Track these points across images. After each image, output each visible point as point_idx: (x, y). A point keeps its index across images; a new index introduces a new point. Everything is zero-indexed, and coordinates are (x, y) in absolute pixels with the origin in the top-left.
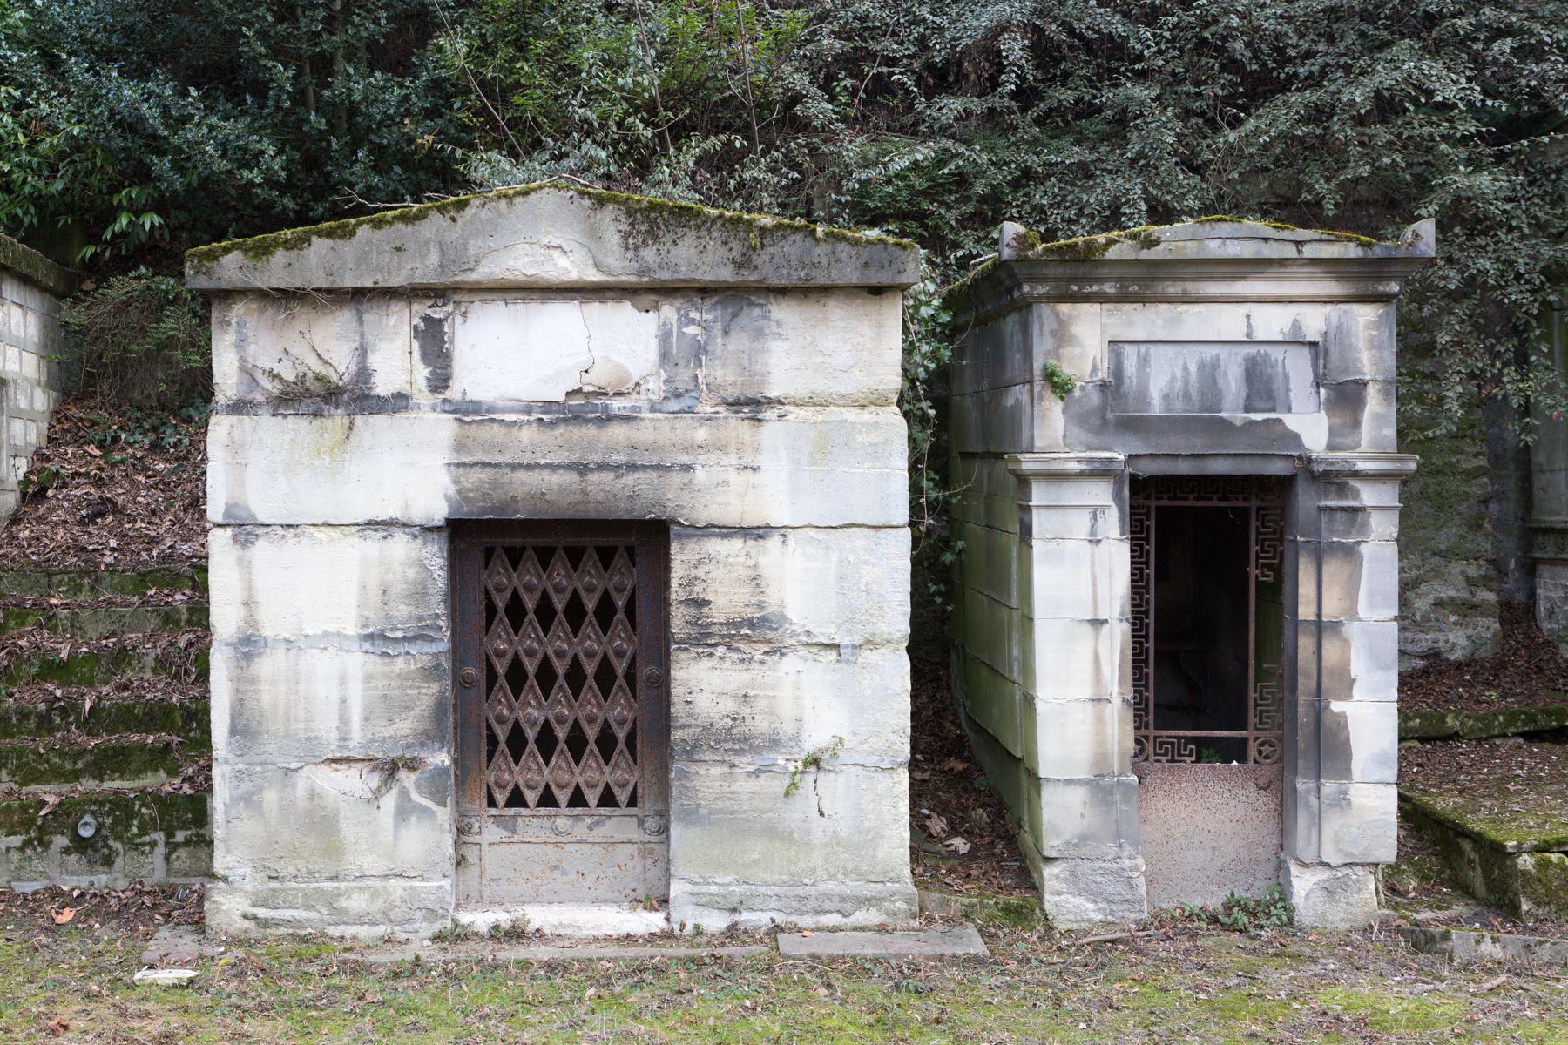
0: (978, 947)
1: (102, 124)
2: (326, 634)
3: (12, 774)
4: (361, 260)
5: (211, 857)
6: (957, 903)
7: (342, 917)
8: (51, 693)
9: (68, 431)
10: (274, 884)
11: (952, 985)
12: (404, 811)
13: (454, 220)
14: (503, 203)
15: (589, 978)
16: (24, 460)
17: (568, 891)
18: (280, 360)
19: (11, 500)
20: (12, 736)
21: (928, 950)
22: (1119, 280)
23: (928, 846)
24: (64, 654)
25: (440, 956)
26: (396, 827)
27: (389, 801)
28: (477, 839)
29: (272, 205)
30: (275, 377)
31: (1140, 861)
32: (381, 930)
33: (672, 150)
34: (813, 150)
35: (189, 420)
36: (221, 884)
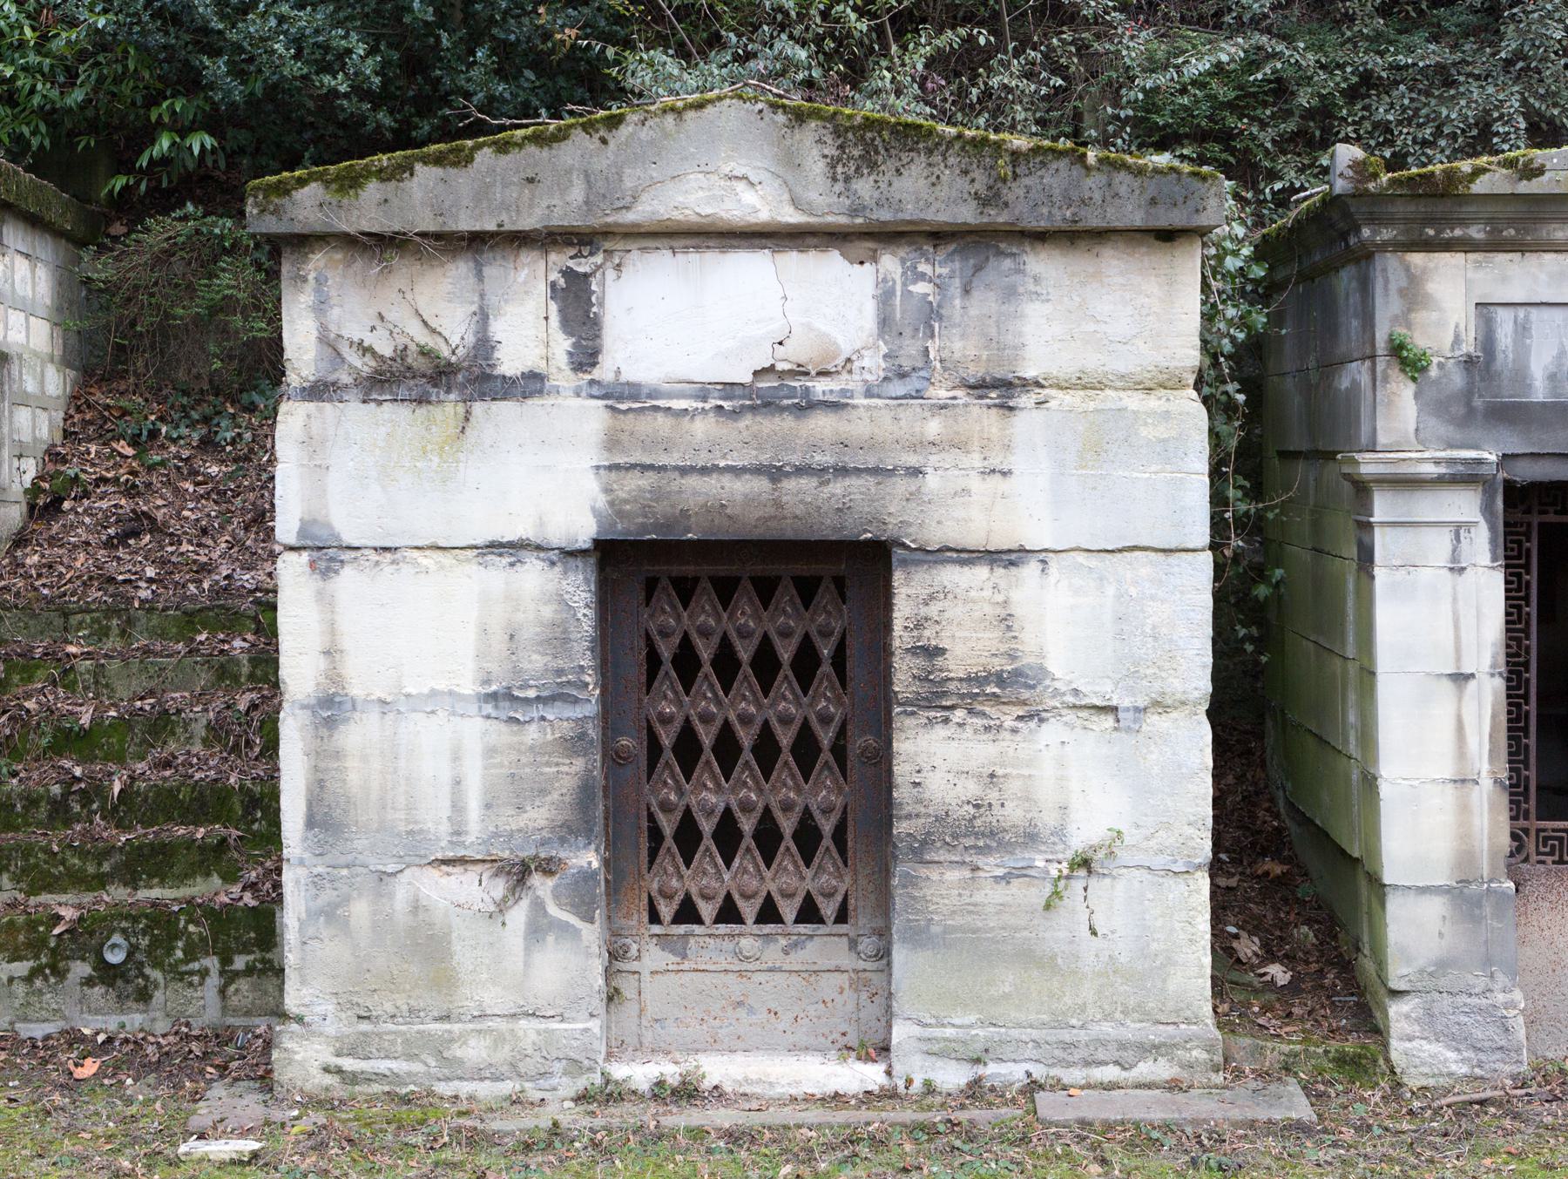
0: (1302, 1109)
1: (136, 14)
2: (434, 693)
3: (16, 879)
4: (482, 195)
5: (281, 990)
6: (1275, 1052)
7: (455, 1069)
8: (68, 771)
9: (91, 423)
10: (365, 1026)
11: (1268, 1161)
12: (538, 929)
13: (604, 141)
14: (670, 119)
15: (784, 1151)
16: (32, 461)
17: (755, 1034)
18: (373, 328)
19: (15, 514)
20: (17, 829)
21: (1236, 1114)
22: (1490, 221)
23: (1235, 976)
24: (85, 720)
25: (586, 1122)
26: (528, 950)
27: (518, 915)
28: (635, 966)
29: (362, 121)
30: (366, 350)
31: (1518, 995)
32: (508, 1087)
33: (894, 48)
34: (1082, 49)
35: (251, 408)
36: (294, 1027)
